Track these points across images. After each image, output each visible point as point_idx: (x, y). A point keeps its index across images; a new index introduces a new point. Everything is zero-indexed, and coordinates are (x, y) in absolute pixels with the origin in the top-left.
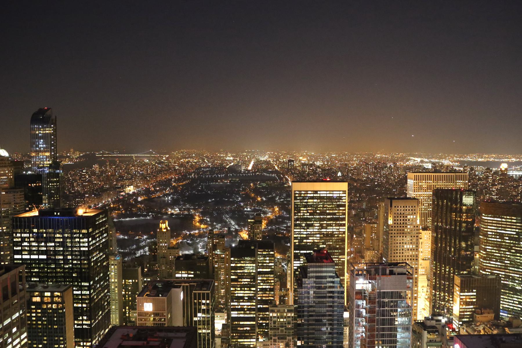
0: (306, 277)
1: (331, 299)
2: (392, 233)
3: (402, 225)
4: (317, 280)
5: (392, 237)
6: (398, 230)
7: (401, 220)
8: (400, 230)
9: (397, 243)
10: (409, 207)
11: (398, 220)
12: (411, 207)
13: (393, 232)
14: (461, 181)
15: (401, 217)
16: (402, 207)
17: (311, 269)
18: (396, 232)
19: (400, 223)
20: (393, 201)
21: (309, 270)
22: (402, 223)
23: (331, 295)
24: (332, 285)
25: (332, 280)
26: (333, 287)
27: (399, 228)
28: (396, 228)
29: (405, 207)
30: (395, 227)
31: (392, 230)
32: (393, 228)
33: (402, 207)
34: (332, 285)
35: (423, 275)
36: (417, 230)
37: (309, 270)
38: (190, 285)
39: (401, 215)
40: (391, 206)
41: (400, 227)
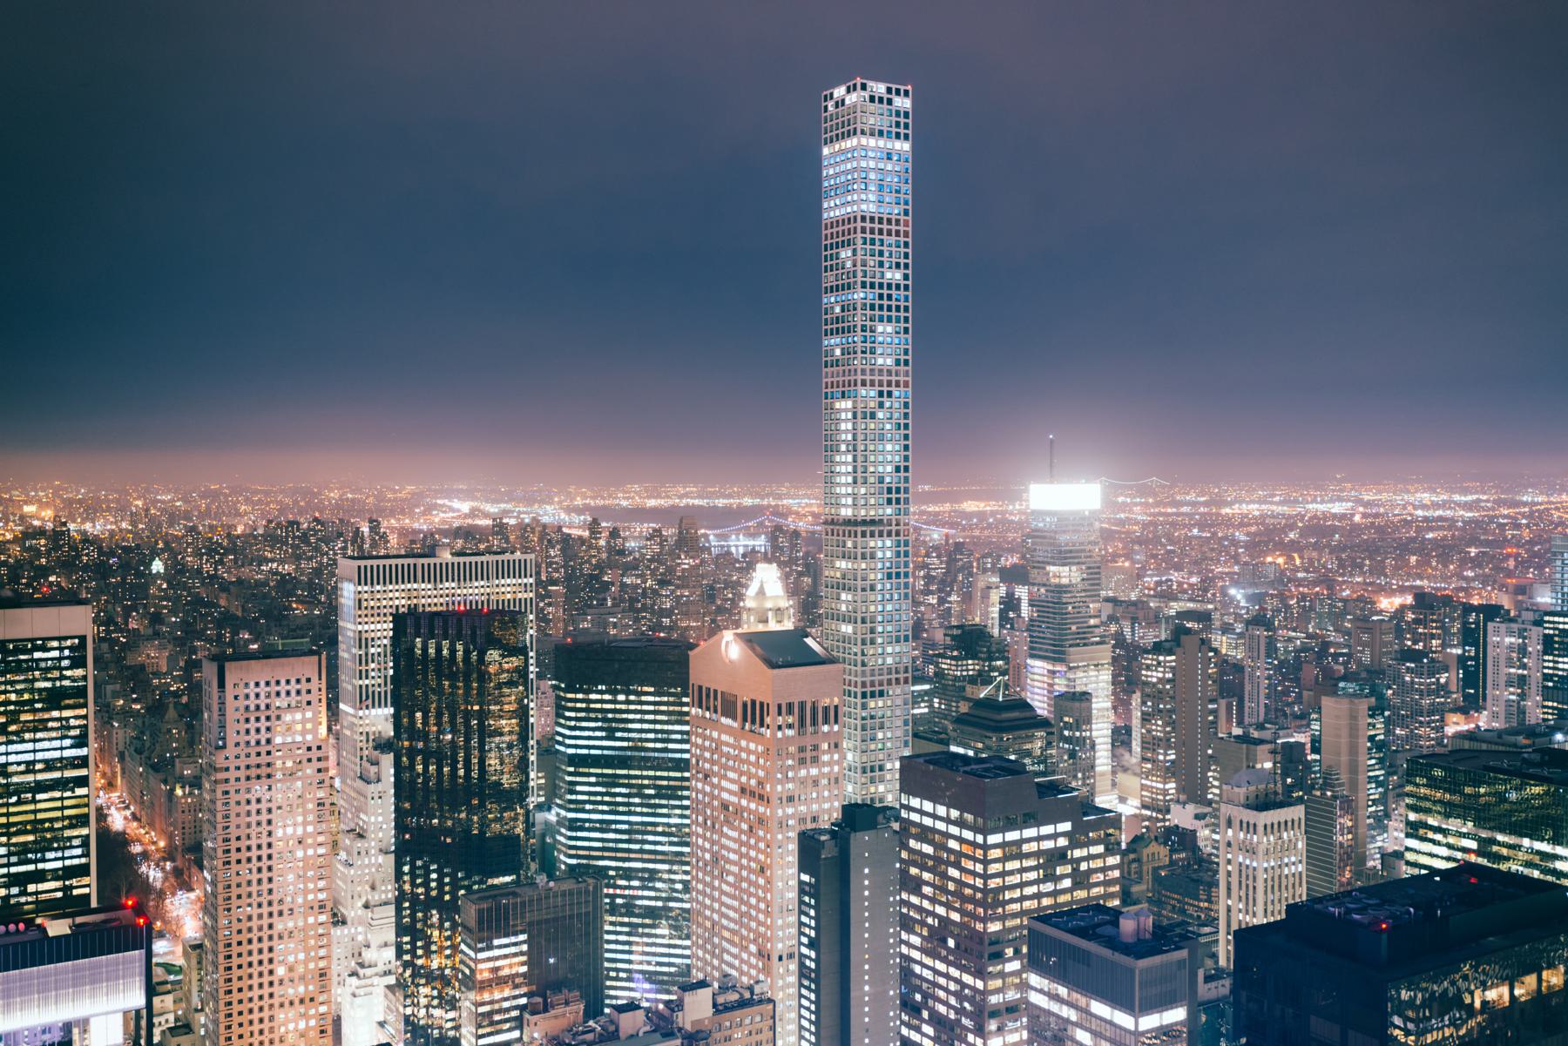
2: (227, 781)
3: (263, 750)
5: (227, 793)
6: (248, 767)
7: (258, 730)
8: (258, 766)
10: (288, 682)
12: (293, 682)
13: (232, 775)
14: (514, 581)
15: (258, 719)
16: (262, 684)
18: (242, 774)
19: (258, 743)
20: (227, 664)
22: (263, 742)
27: (254, 760)
29: (273, 683)
31: (227, 769)
33: (262, 684)
35: (386, 903)
36: (319, 759)
39: (258, 714)
40: (222, 685)
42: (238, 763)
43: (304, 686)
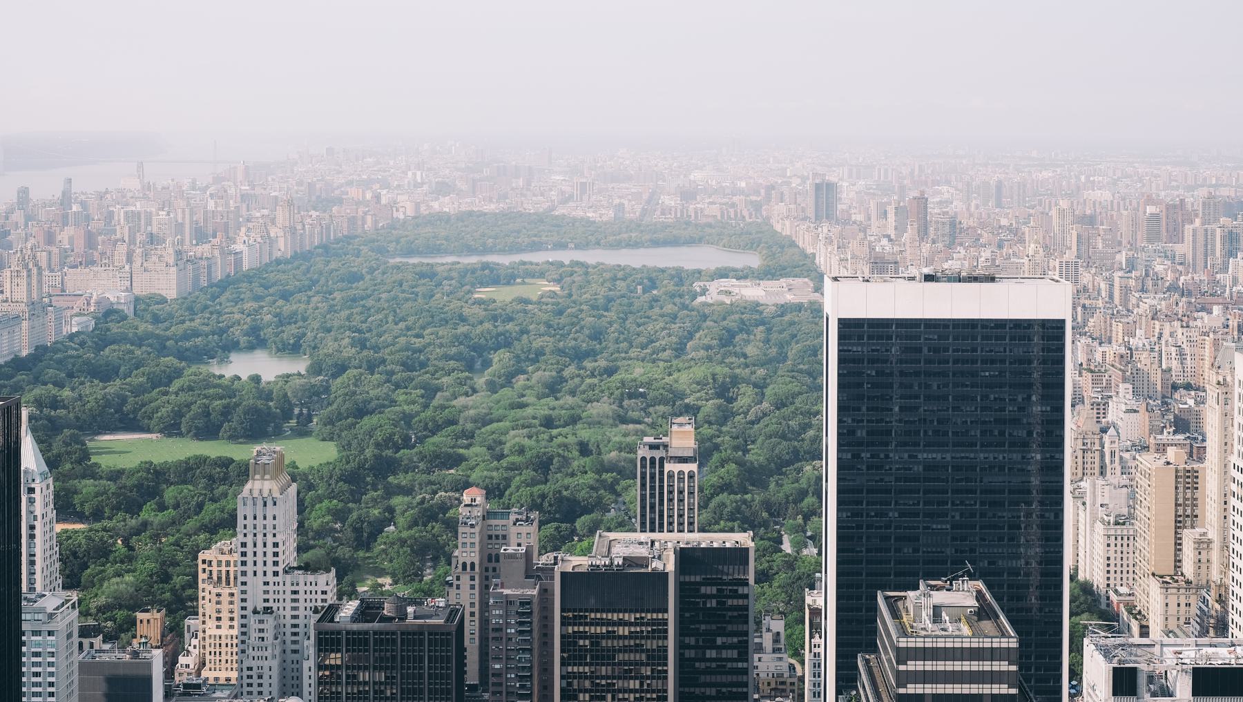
17: (912, 666)
21: (902, 668)
37: (902, 668)
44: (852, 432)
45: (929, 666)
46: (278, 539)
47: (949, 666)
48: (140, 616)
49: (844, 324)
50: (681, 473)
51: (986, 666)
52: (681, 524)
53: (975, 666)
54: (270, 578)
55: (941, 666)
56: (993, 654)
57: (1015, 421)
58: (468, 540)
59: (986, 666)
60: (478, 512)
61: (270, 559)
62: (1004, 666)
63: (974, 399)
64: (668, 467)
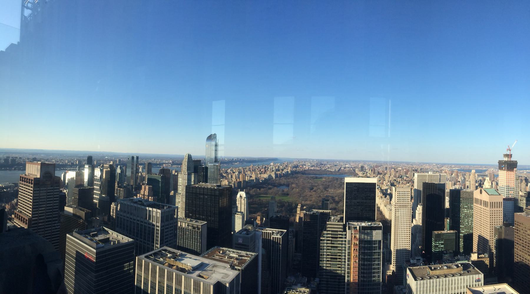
0: (325, 230)
1: (341, 245)
2: (396, 207)
4: (332, 233)
5: (396, 209)
6: (399, 205)
9: (399, 213)
11: (399, 199)
13: (397, 206)
17: (328, 226)
21: (327, 226)
23: (341, 242)
24: (341, 236)
25: (341, 233)
26: (342, 238)
27: (400, 204)
28: (398, 204)
30: (398, 203)
31: (396, 205)
32: (397, 204)
34: (341, 236)
36: (410, 205)
37: (327, 226)
38: (272, 232)
41: (401, 203)
42: (398, 204)
43: (408, 193)
44: (347, 198)
45: (331, 226)
46: (274, 208)
47: (334, 226)
48: (258, 217)
49: (346, 183)
50: (327, 203)
51: (339, 226)
52: (326, 209)
53: (337, 226)
54: (273, 213)
55: (332, 226)
56: (340, 225)
57: (369, 196)
58: (298, 210)
59: (339, 226)
60: (300, 206)
61: (273, 211)
62: (341, 227)
63: (364, 193)
64: (325, 202)
